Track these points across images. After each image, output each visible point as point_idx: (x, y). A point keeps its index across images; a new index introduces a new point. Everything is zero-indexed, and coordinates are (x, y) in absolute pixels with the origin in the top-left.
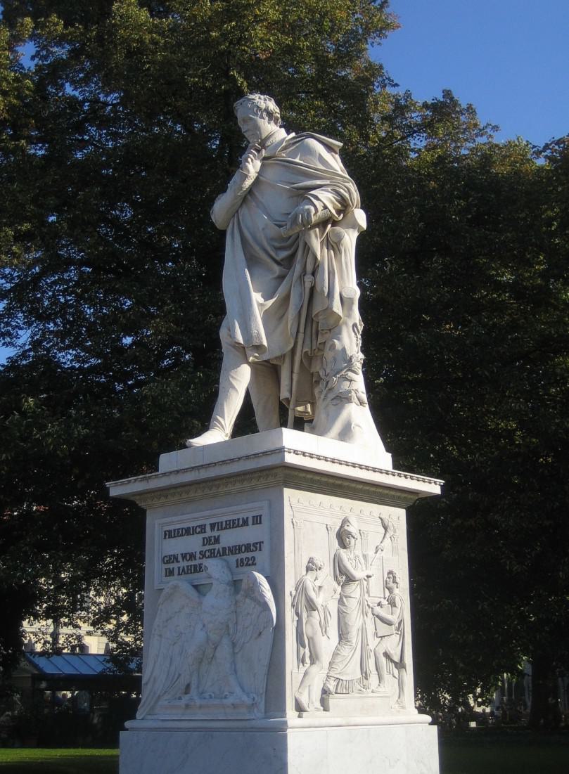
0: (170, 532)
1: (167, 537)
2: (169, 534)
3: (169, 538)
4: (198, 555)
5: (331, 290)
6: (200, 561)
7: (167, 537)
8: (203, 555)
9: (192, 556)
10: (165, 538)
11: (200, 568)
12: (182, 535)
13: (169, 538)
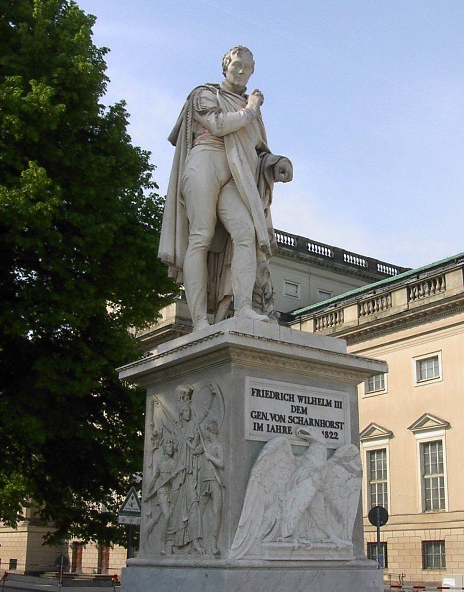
0: (259, 391)
1: (255, 394)
2: (256, 392)
3: (257, 396)
4: (287, 419)
5: (187, 230)
6: (289, 425)
7: (255, 394)
8: (292, 420)
9: (281, 418)
10: (253, 395)
11: (289, 430)
12: (271, 397)
13: (257, 396)
